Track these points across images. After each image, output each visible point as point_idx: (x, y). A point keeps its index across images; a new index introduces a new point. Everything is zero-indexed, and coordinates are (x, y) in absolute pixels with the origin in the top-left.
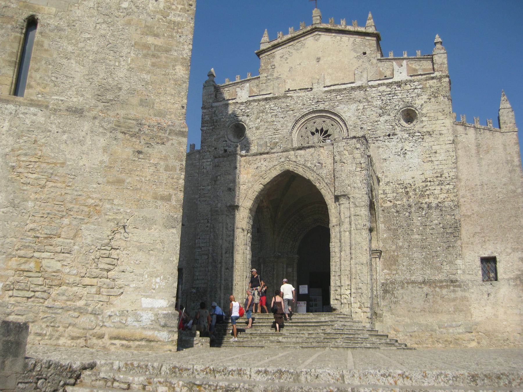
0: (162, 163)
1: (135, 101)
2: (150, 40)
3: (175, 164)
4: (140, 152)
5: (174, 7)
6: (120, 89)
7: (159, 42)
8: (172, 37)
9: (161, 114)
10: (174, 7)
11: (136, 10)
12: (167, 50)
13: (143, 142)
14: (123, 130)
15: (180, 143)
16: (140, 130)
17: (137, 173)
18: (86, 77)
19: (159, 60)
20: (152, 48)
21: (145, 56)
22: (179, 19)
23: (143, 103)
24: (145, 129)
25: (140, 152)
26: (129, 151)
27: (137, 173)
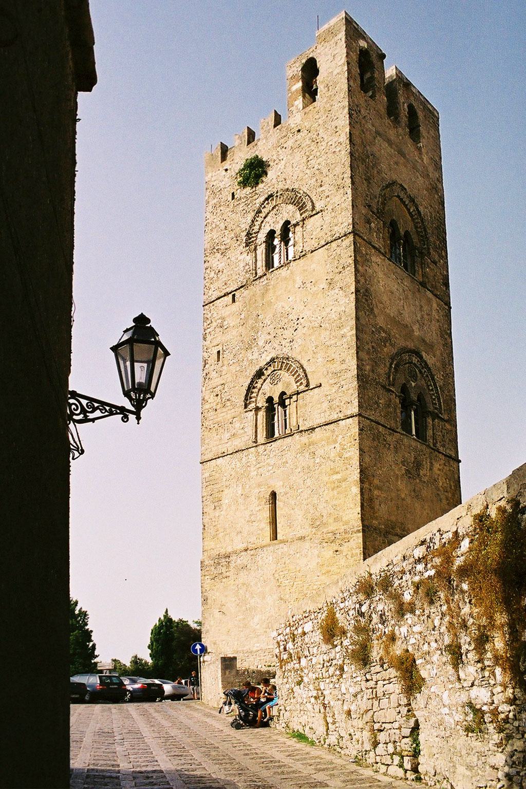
0: (349, 553)
1: (331, 520)
2: (335, 477)
3: (357, 551)
4: (337, 551)
5: (345, 447)
6: (322, 516)
7: (338, 476)
8: (347, 469)
9: (346, 523)
10: (345, 447)
11: (323, 461)
12: (345, 480)
13: (338, 544)
14: (326, 541)
15: (358, 537)
16: (335, 538)
17: (337, 564)
18: (304, 517)
19: (341, 488)
20: (336, 482)
21: (333, 489)
22: (349, 454)
23: (336, 520)
24: (338, 536)
25: (337, 551)
26: (331, 553)
27: (337, 564)
